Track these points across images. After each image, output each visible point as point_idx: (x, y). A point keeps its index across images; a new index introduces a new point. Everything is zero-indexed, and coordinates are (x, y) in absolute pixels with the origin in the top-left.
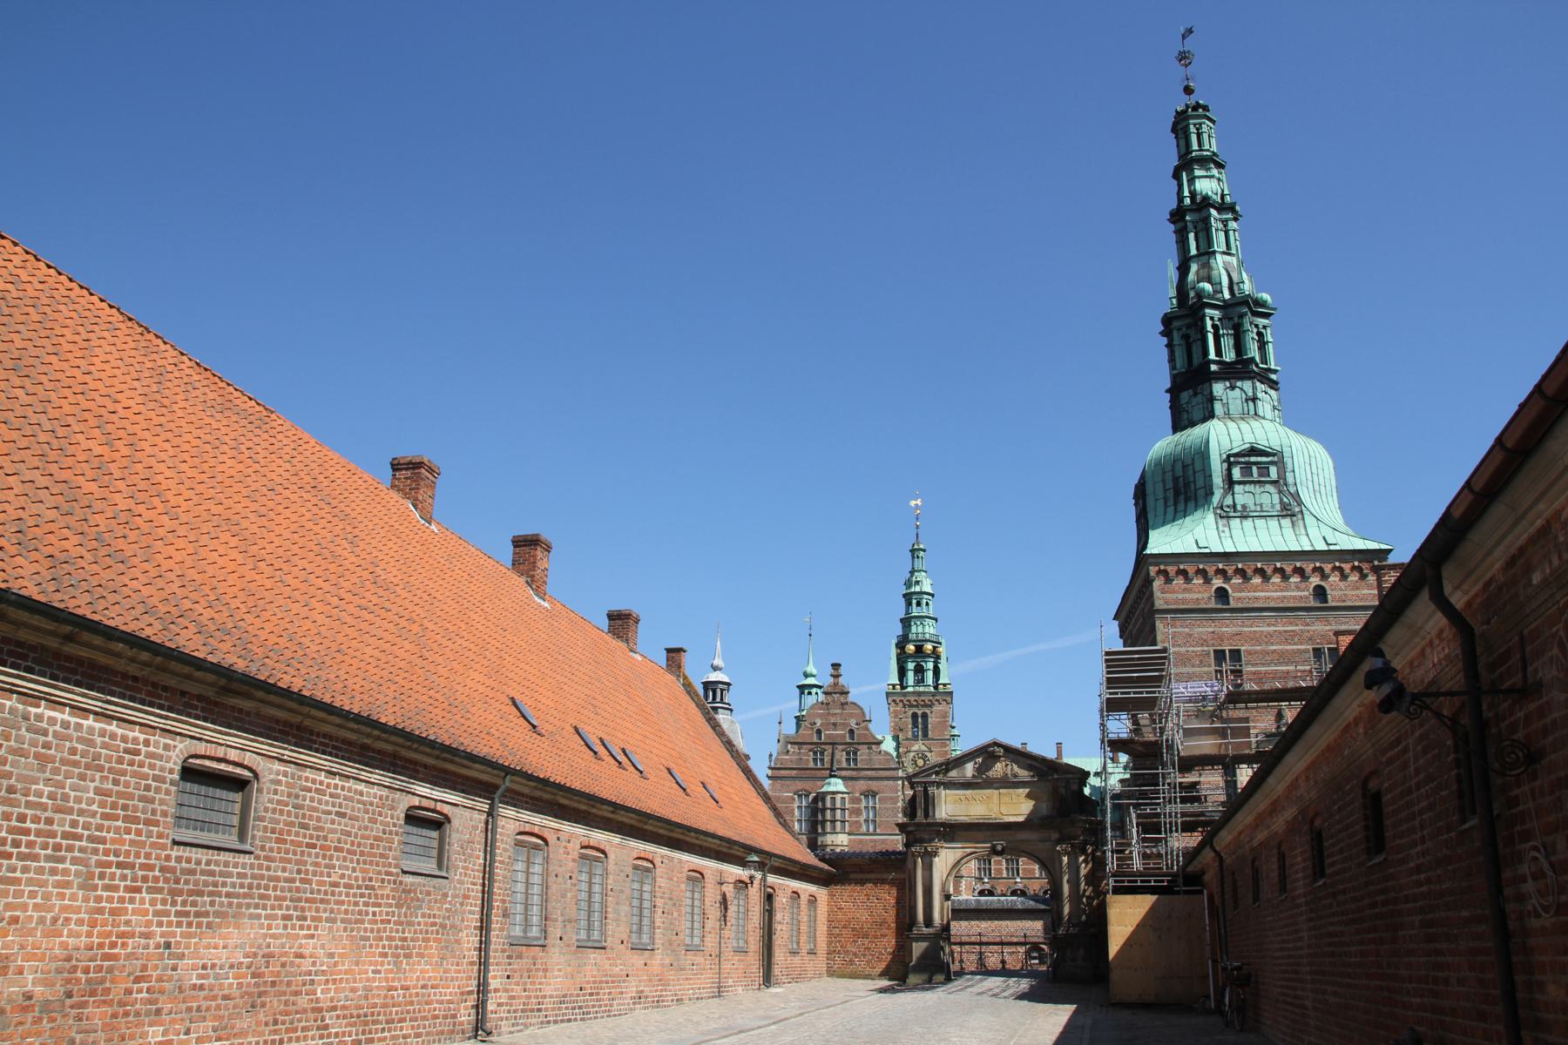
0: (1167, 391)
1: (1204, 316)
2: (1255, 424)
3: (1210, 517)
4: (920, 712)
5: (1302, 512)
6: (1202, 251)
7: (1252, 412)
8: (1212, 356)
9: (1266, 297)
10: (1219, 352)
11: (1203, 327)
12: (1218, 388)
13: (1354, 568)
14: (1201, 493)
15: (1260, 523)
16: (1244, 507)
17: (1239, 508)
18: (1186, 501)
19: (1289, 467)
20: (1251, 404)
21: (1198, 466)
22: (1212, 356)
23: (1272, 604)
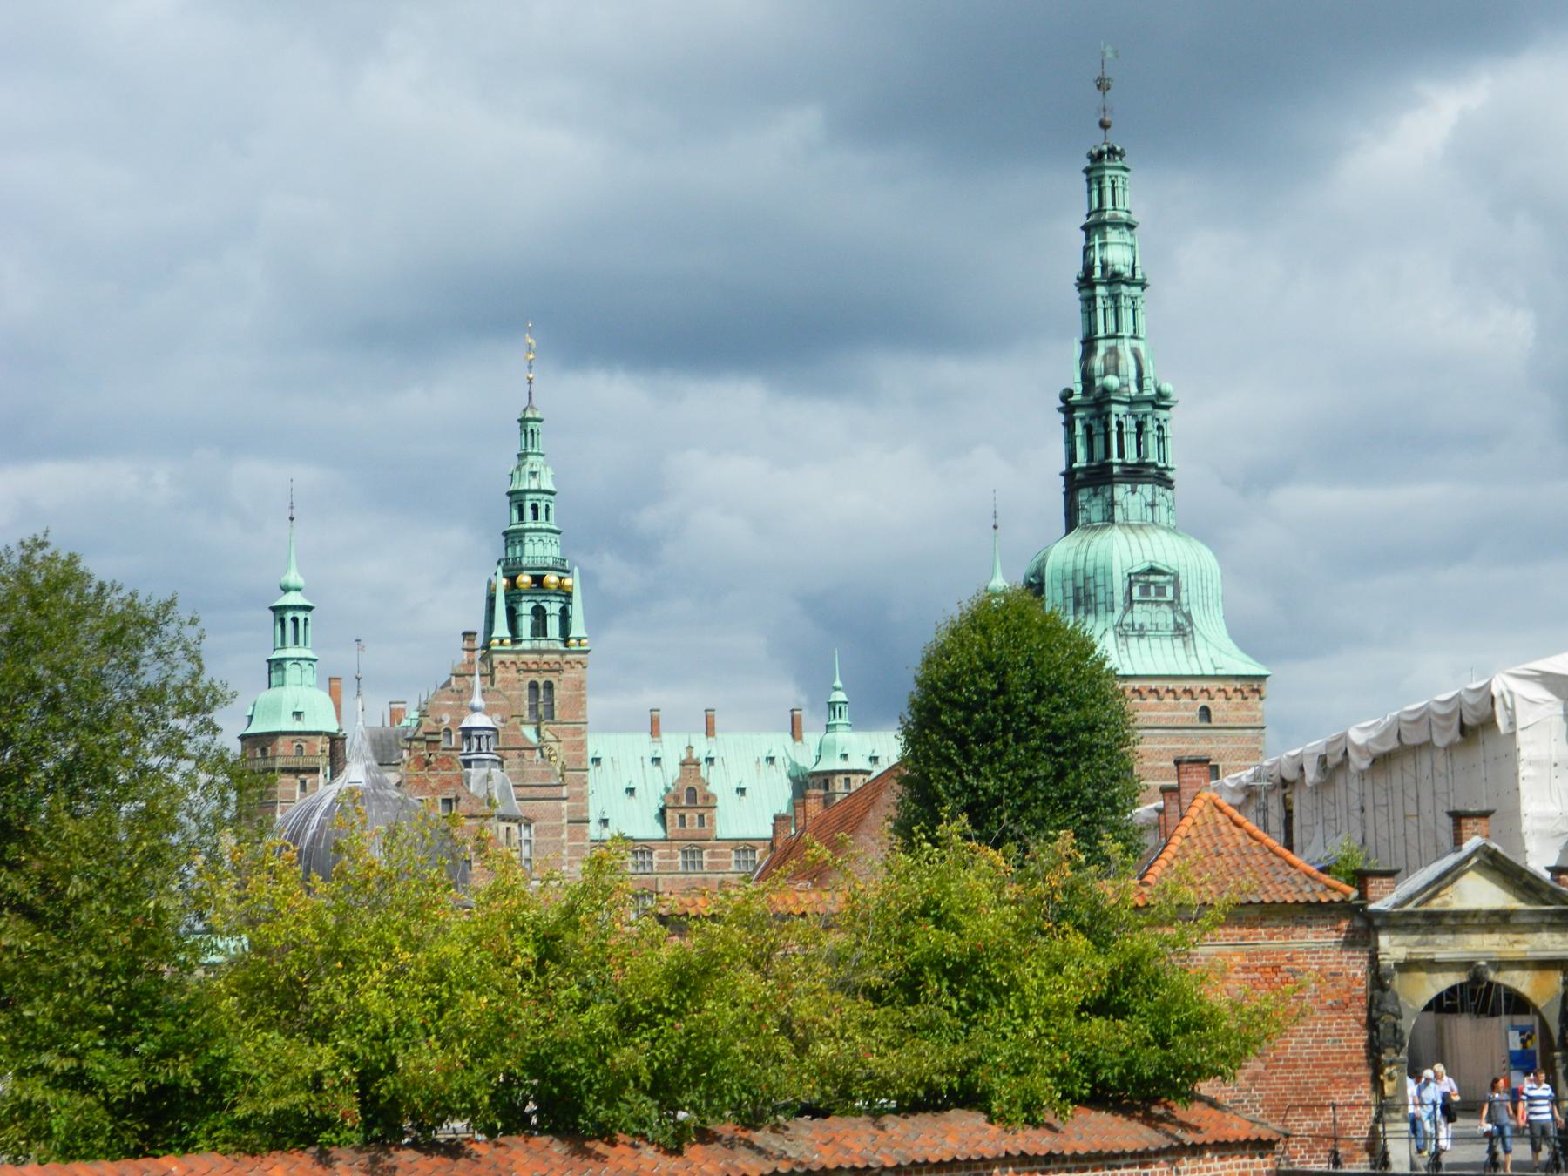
0: (1062, 474)
2: (1153, 537)
4: (541, 682)
5: (1192, 632)
7: (1150, 519)
9: (1167, 387)
10: (1121, 454)
11: (1107, 425)
12: (1120, 492)
13: (1236, 690)
14: (1101, 608)
15: (1155, 642)
16: (1141, 626)
17: (1137, 627)
18: (1087, 612)
19: (1184, 587)
20: (1149, 509)
21: (1100, 580)
22: (1115, 459)
23: (1163, 723)
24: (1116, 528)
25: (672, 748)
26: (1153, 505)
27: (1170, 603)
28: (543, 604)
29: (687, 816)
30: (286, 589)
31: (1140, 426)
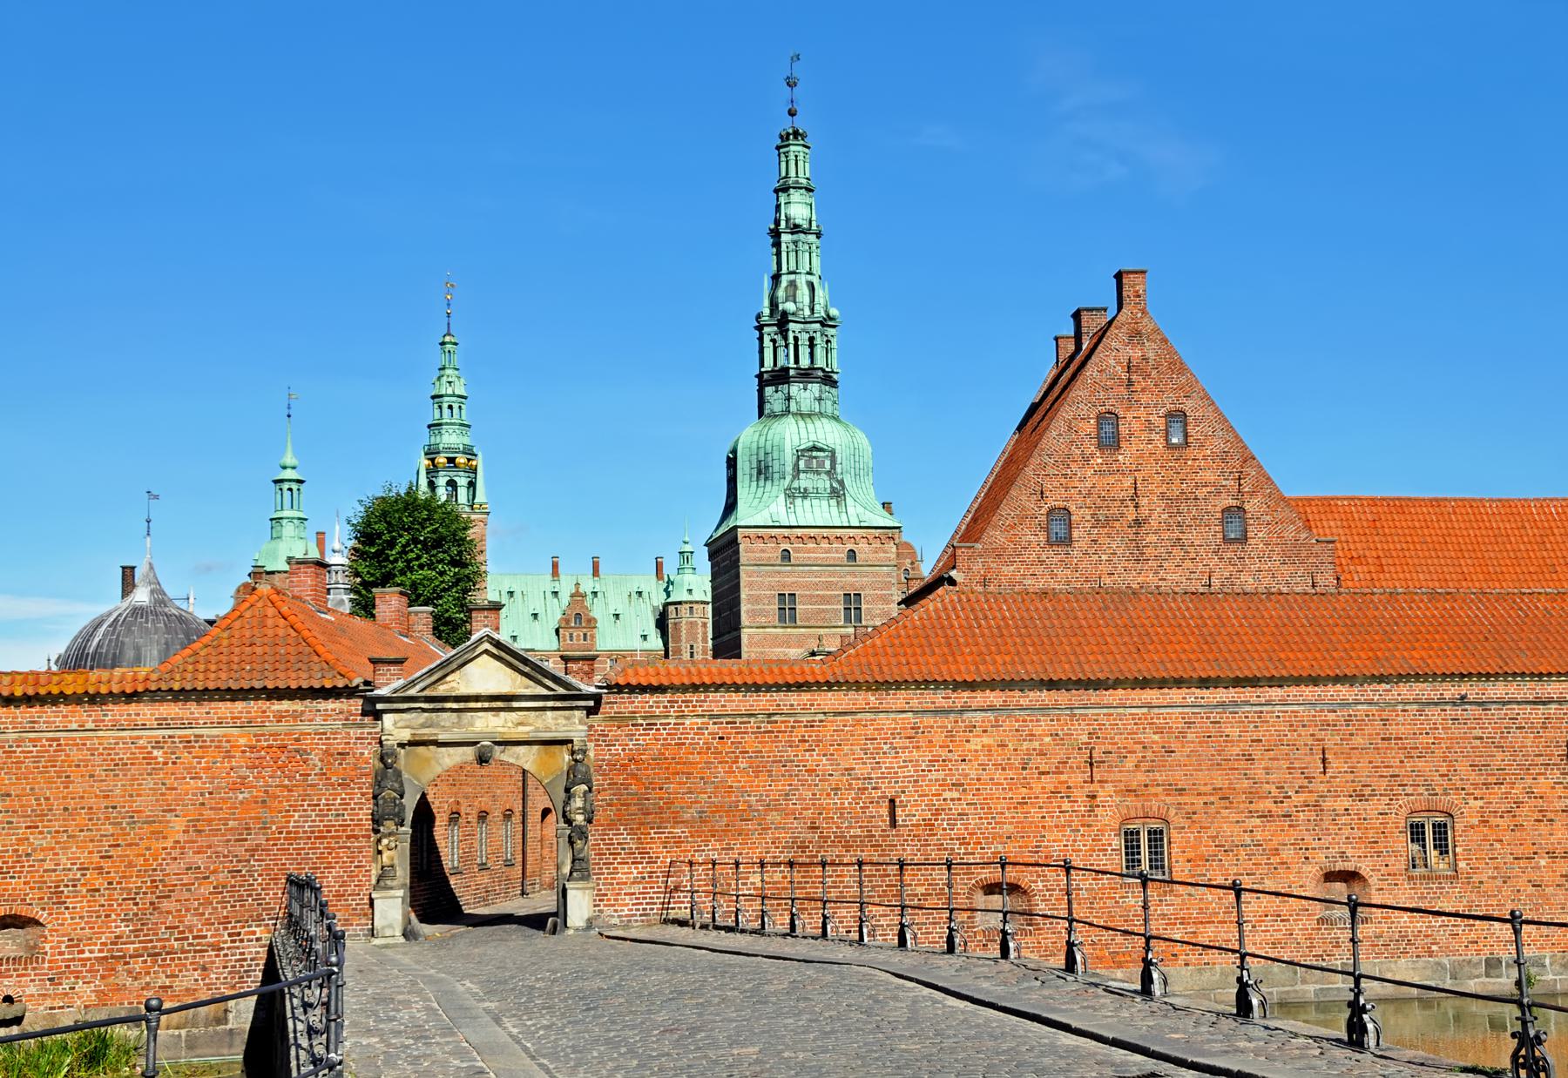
1: (788, 330)
2: (818, 423)
3: (782, 496)
6: (791, 269)
7: (817, 410)
8: (792, 365)
9: (834, 312)
10: (797, 361)
11: (785, 338)
12: (795, 389)
14: (776, 476)
15: (816, 502)
16: (805, 489)
17: (802, 490)
18: (766, 479)
23: (819, 562)
24: (790, 416)
25: (566, 589)
26: (820, 399)
27: (828, 473)
28: (455, 478)
29: (575, 634)
30: (284, 468)
31: (811, 339)
